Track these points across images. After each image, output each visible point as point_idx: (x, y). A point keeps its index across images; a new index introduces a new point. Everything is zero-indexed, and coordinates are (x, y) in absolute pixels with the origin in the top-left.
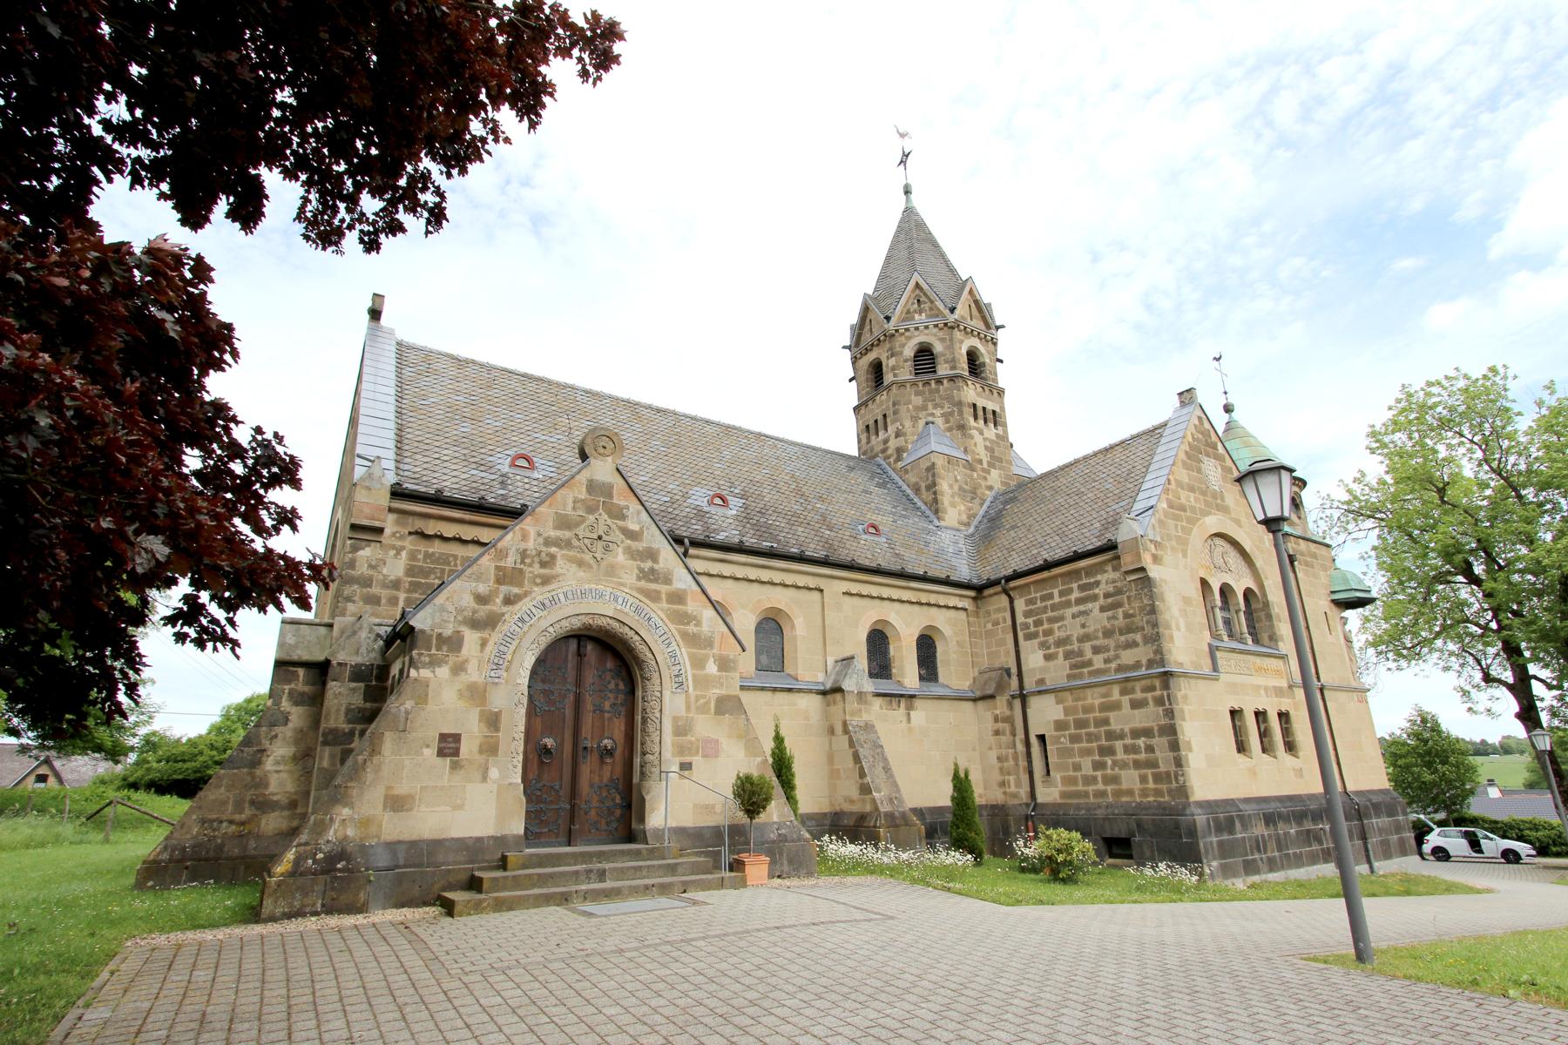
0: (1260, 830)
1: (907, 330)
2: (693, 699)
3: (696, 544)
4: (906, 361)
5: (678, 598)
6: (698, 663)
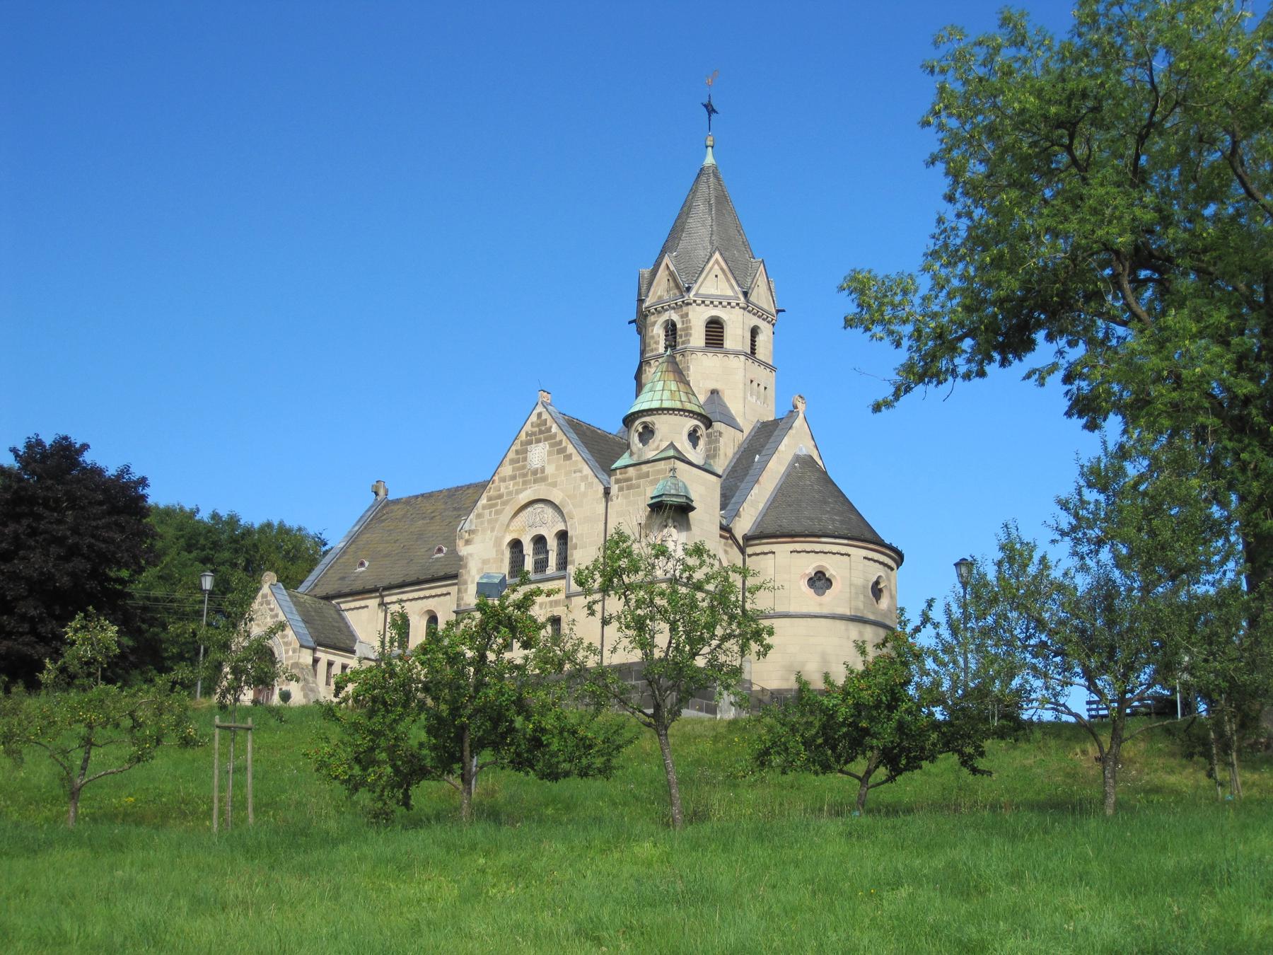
3: (385, 589)
6: (287, 652)
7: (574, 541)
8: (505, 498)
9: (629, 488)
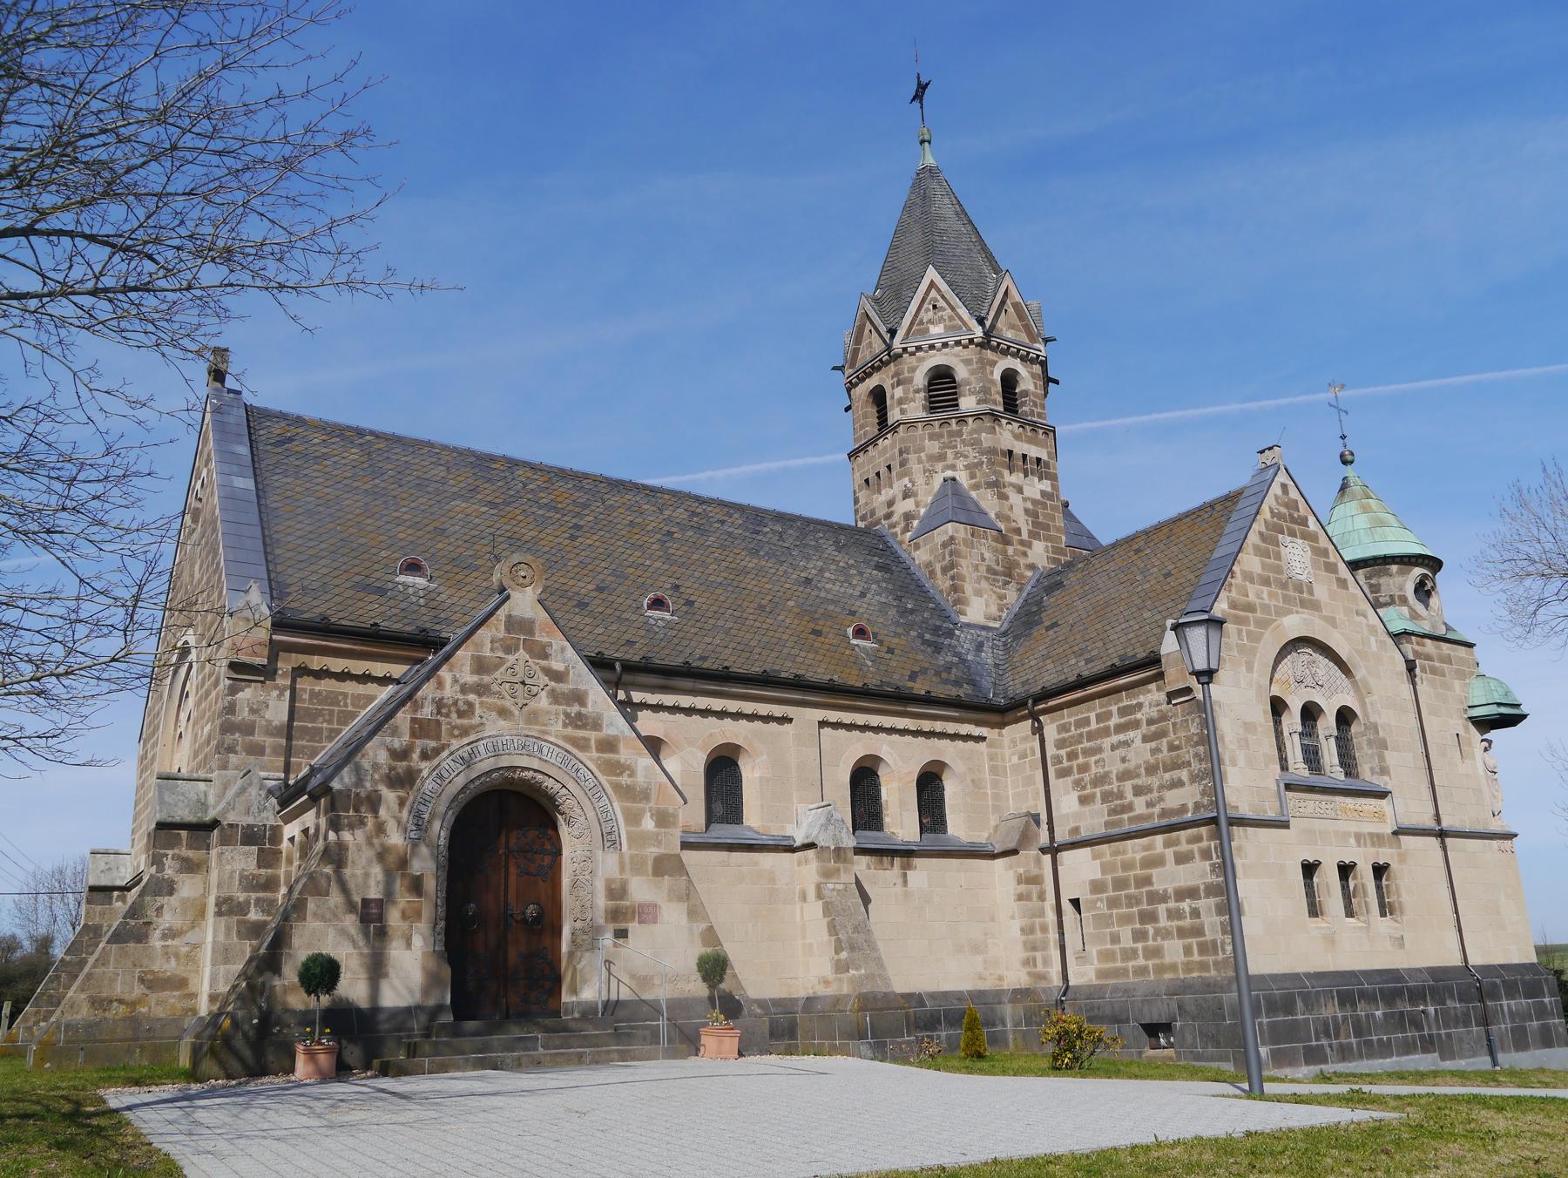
0: (1331, 1010)
1: (919, 348)
2: (627, 859)
4: (917, 391)
5: (609, 745)
6: (633, 818)
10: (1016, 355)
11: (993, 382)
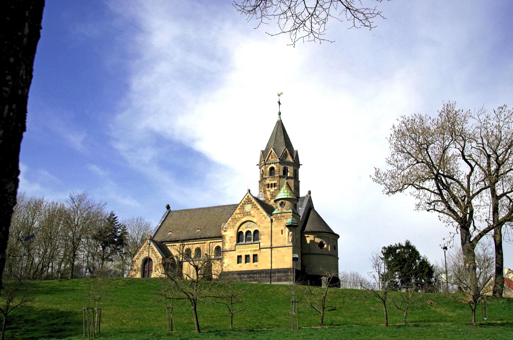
5: (155, 253)
7: (261, 233)
8: (237, 219)
9: (278, 219)
10: (273, 163)
11: (267, 171)
